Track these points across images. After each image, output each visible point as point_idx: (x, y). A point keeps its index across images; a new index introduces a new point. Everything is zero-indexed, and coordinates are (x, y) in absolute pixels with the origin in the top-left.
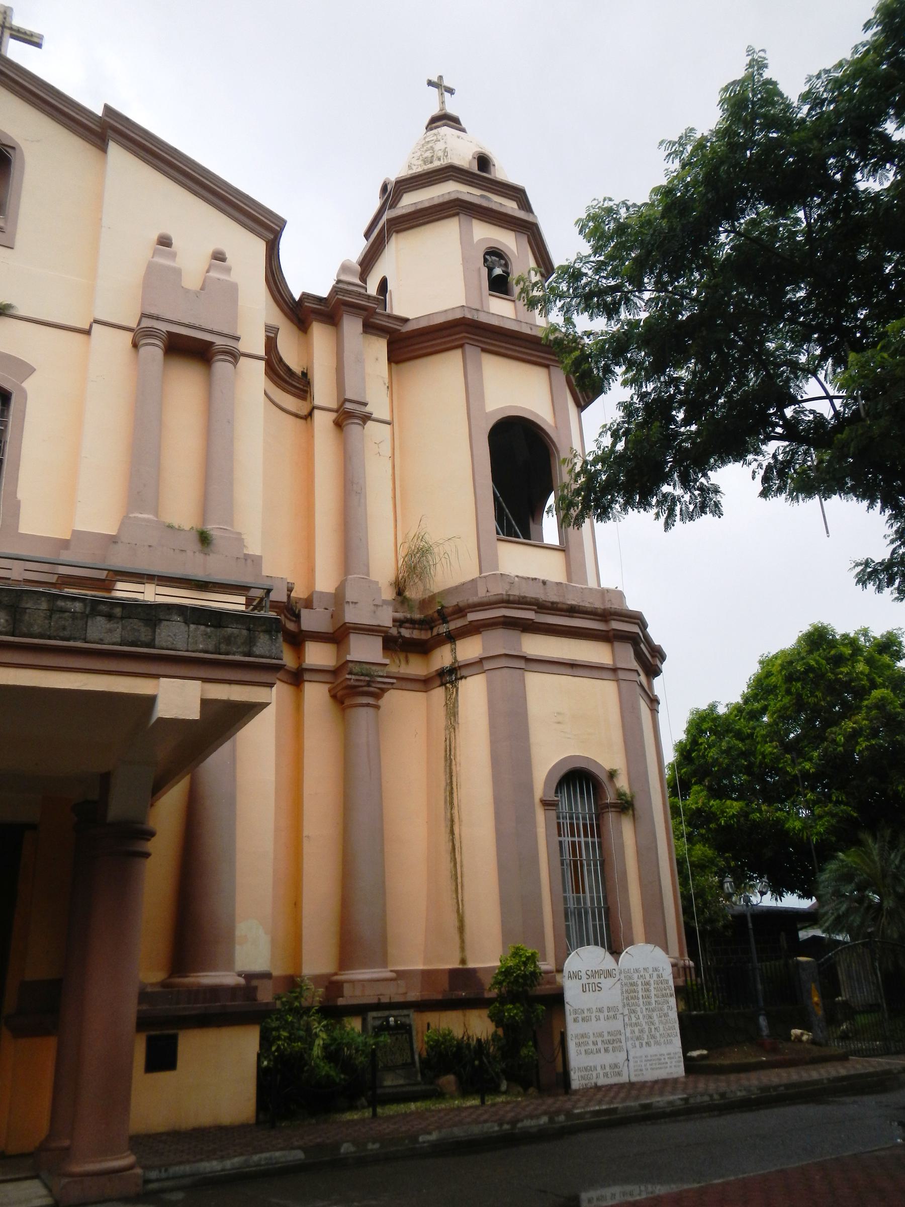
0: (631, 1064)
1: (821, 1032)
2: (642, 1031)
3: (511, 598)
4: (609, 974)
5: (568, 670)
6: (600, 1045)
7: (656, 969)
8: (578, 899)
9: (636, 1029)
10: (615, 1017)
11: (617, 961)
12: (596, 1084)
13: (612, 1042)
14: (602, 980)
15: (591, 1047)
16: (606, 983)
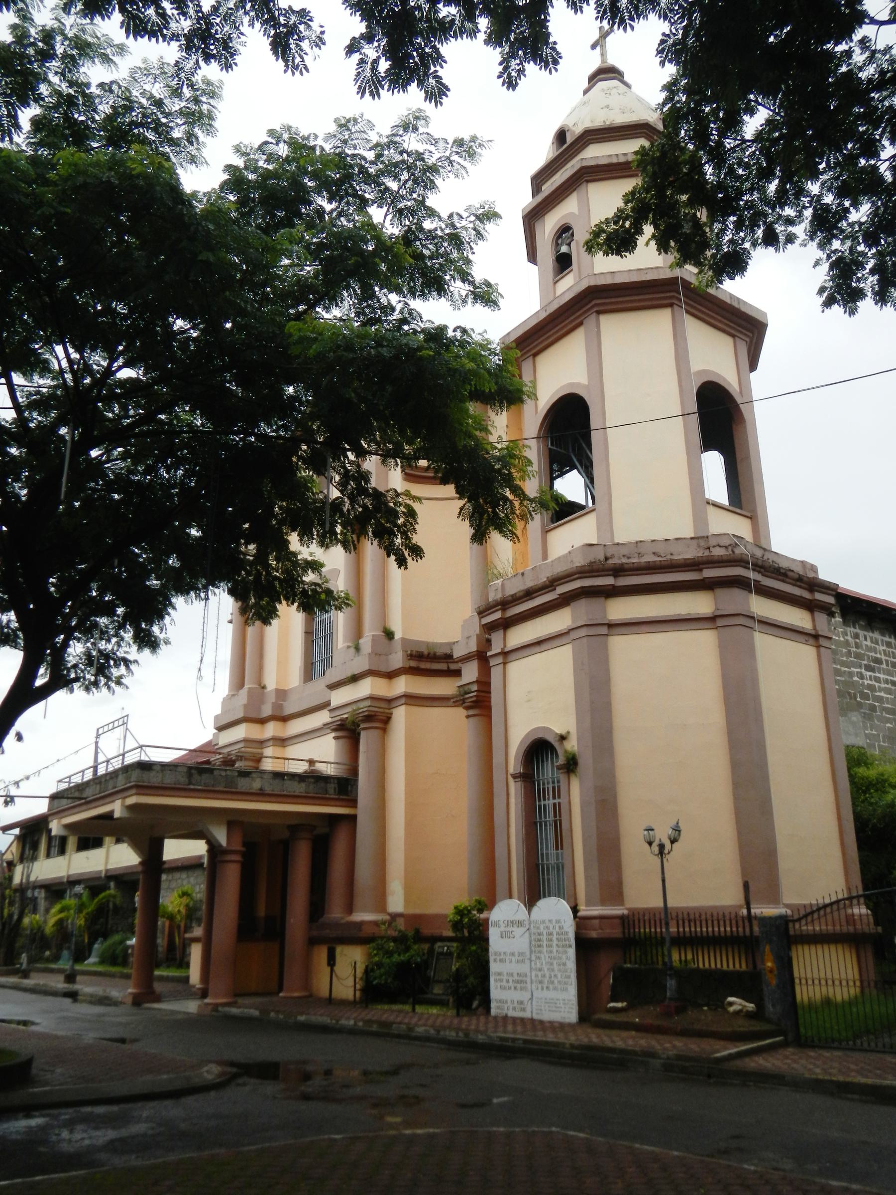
0: (534, 1003)
1: (773, 1006)
2: (544, 976)
3: (481, 609)
4: (520, 924)
5: (537, 649)
6: (511, 984)
7: (558, 922)
8: (557, 855)
9: (540, 974)
10: (523, 961)
11: (530, 911)
12: (506, 1016)
13: (520, 982)
14: (515, 929)
15: (504, 983)
16: (518, 931)
